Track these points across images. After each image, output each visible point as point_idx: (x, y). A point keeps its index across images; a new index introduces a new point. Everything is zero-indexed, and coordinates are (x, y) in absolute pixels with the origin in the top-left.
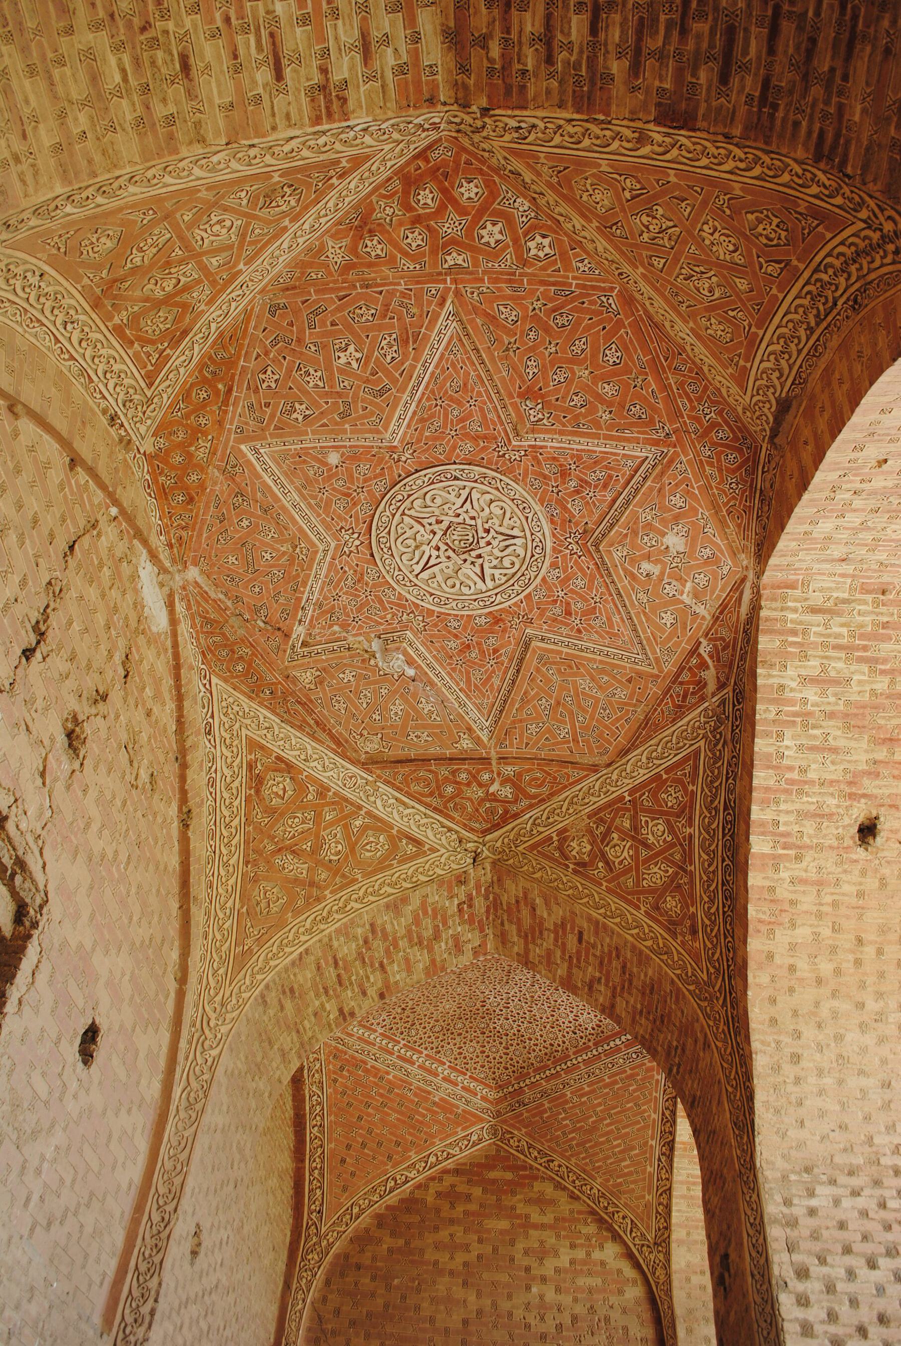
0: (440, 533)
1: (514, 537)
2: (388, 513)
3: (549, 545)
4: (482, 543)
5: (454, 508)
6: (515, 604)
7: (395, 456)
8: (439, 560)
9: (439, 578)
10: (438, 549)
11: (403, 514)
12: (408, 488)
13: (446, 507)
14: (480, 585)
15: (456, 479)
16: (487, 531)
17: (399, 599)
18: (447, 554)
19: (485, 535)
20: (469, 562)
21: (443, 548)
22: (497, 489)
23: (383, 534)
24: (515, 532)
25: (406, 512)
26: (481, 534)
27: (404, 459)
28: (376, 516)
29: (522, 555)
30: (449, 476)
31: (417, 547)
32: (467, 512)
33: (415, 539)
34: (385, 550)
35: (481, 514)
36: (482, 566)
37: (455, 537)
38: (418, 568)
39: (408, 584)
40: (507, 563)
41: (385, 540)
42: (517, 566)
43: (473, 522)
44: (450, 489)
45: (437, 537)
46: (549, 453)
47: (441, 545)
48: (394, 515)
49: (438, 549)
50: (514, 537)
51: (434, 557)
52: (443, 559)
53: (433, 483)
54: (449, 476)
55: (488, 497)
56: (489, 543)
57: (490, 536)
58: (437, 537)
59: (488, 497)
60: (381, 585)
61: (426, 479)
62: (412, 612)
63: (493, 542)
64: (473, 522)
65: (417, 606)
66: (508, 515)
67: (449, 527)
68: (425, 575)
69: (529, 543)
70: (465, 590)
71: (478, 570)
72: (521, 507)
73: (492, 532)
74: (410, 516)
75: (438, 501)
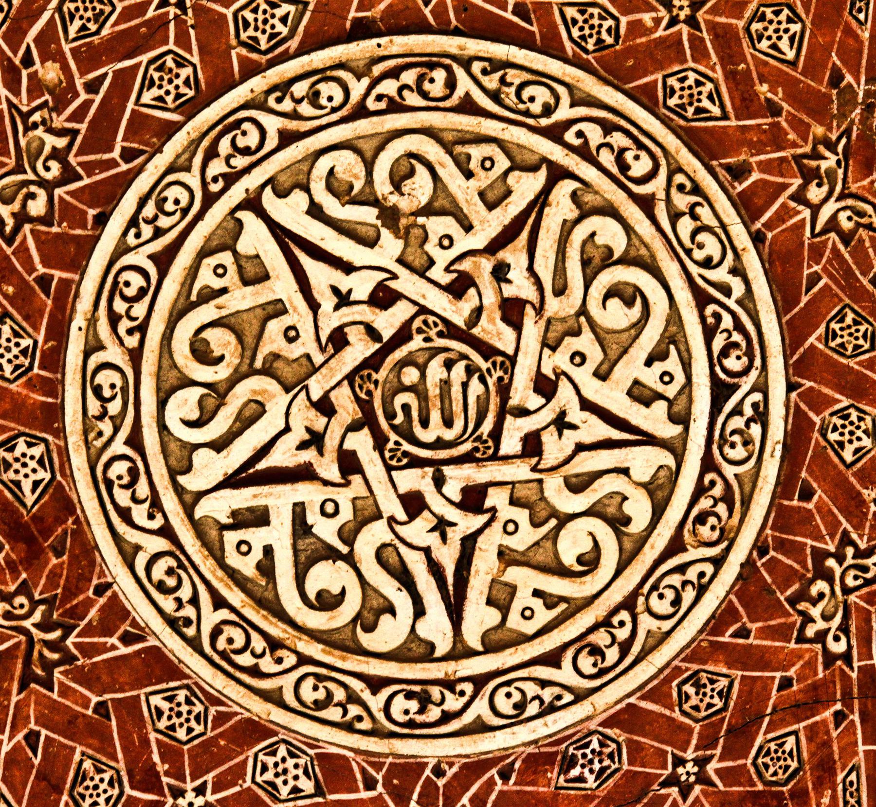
0: (458, 313)
1: (455, 612)
2: (564, 112)
3: (429, 750)
4: (410, 480)
5: (583, 376)
6: (116, 612)
7: (829, 162)
8: (327, 302)
9: (241, 299)
10: (384, 297)
11: (558, 173)
12: (682, 201)
13: (586, 342)
14: (208, 468)
15: (721, 391)
16: (473, 499)
17: (140, 124)
18: (354, 334)
19: (453, 490)
20: (319, 423)
21: (387, 322)
22: (676, 546)
23: (464, 84)
24: (479, 618)
25: (566, 187)
26: (457, 478)
27: (815, 194)
28: (554, 67)
29: (366, 640)
30: (733, 363)
31: (390, 216)
32: (561, 423)
33: (428, 210)
34: (389, 87)
35: (553, 486)
36: (304, 474)
37: (435, 371)
38: (290, 212)
39: (217, 167)
40: (325, 576)
41: (437, 89)
42: (316, 620)
43: (511, 444)
44: (673, 364)
45: (439, 302)
46: (849, 750)
47: (401, 312)
48: (555, 133)
49: (384, 297)
50: (455, 612)
51: (344, 282)
52: (330, 320)
53: (702, 299)
54: (733, 363)
55: (639, 509)
56: (414, 504)
57: (452, 514)
58: (439, 302)
59: (639, 509)
60: (214, 51)
61: (720, 274)
62: (69, 175)
63: (424, 521)
64: (511, 444)
65: (108, 195)
66: (556, 586)
67: (487, 351)
68: (255, 238)
69: (435, 671)
70: (184, 404)
71: (283, 456)
72: (601, 638)
73: (468, 523)
74: (541, 201)
75: (616, 316)
